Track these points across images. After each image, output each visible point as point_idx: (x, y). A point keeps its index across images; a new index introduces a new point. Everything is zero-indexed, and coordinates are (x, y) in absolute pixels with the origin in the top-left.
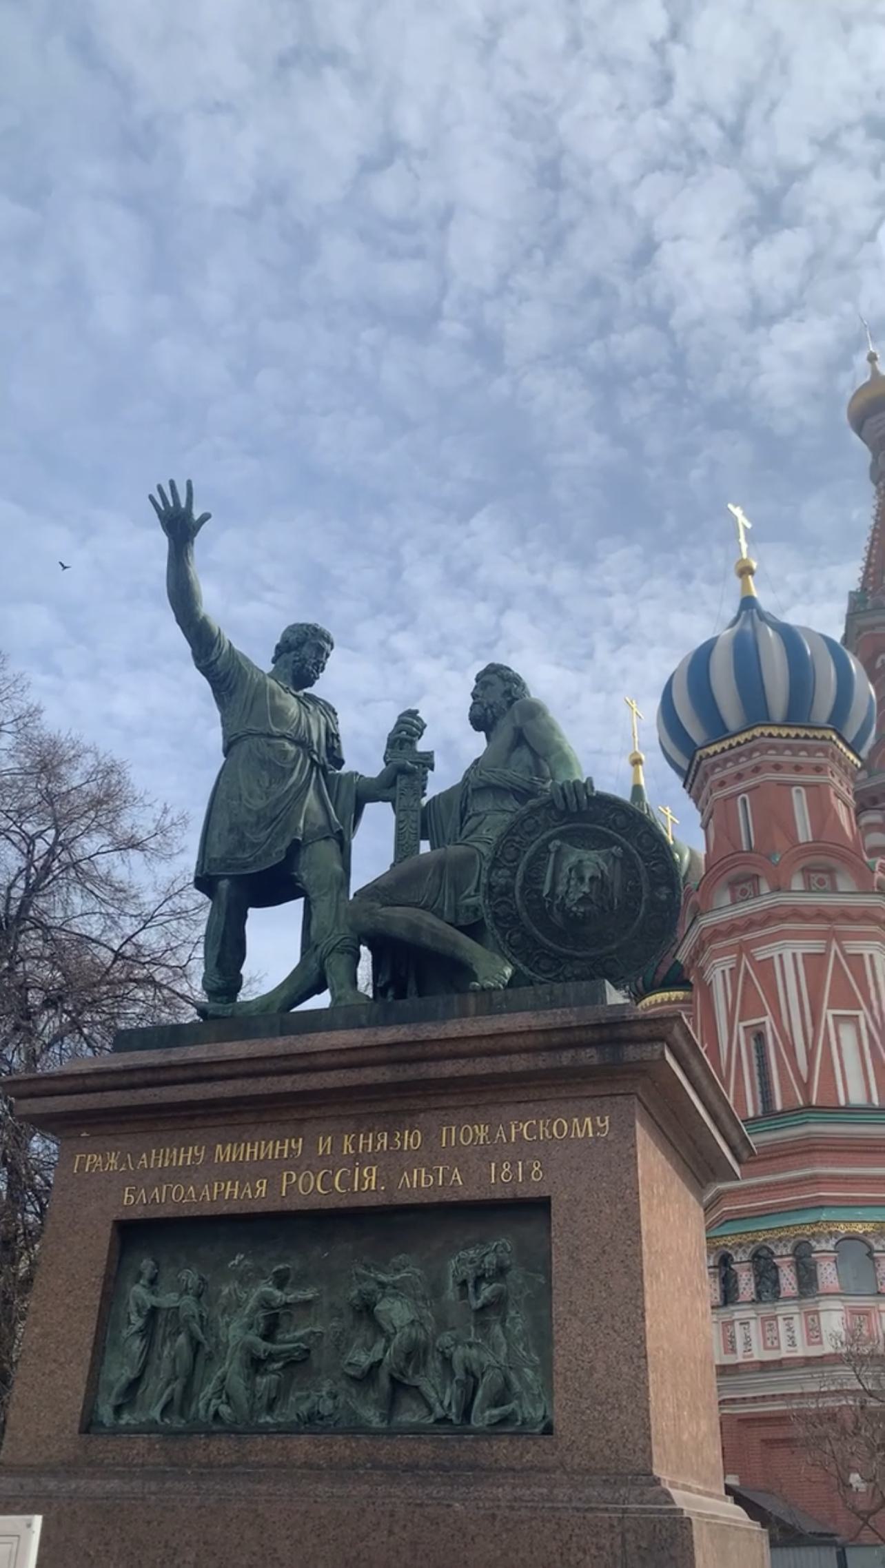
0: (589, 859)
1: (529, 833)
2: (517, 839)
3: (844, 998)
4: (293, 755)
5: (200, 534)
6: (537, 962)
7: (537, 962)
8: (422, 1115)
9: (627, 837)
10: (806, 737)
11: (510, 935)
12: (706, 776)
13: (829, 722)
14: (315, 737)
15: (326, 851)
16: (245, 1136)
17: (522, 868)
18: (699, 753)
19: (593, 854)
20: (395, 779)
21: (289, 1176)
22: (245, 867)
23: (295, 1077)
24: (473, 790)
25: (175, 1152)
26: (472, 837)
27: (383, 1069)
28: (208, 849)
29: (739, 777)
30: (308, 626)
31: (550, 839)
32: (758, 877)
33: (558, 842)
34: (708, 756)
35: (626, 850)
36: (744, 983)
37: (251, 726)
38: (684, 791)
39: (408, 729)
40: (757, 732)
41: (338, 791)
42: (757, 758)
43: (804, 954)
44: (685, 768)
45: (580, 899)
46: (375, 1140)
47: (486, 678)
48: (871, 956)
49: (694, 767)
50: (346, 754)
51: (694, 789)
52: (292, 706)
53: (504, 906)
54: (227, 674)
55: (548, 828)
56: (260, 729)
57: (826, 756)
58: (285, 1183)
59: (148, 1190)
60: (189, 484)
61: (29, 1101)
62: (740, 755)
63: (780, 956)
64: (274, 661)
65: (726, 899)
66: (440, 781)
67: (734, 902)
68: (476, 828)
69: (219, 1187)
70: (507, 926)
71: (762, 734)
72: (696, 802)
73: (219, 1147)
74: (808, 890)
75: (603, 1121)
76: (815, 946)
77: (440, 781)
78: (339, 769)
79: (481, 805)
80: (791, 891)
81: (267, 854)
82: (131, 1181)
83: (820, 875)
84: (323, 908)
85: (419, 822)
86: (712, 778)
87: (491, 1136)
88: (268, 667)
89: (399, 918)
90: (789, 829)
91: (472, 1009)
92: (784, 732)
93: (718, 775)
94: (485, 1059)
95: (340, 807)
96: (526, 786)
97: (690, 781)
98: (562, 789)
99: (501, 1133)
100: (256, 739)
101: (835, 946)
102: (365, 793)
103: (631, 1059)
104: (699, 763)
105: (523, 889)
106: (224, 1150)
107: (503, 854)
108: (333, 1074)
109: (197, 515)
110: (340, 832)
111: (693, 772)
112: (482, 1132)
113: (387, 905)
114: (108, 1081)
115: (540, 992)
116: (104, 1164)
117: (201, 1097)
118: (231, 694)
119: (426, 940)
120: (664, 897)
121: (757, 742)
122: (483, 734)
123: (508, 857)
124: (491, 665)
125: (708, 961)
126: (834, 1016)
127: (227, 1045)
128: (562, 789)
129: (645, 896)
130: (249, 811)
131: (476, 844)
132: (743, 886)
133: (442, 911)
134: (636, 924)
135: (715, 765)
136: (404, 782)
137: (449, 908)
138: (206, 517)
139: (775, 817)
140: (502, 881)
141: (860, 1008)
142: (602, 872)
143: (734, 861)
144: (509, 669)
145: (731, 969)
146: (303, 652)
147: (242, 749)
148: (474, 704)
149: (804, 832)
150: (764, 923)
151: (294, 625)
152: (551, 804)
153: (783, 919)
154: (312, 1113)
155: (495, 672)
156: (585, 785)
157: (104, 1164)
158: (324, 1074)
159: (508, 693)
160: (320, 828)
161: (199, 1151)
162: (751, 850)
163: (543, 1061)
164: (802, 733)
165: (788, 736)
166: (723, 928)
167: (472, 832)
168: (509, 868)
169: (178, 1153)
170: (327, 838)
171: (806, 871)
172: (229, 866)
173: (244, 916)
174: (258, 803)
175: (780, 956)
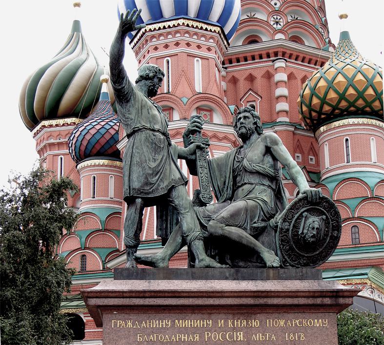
1: (297, 209)
2: (293, 211)
4: (162, 141)
8: (258, 315)
12: (147, 41)
13: (218, 22)
16: (187, 318)
17: (293, 222)
20: (195, 151)
21: (208, 334)
22: (148, 194)
23: (214, 299)
25: (157, 322)
27: (250, 299)
29: (166, 46)
33: (306, 213)
34: (150, 30)
35: (327, 217)
40: (181, 22)
46: (241, 322)
47: (247, 114)
53: (285, 237)
56: (148, 126)
58: (206, 336)
59: (149, 335)
61: (95, 299)
62: (169, 33)
64: (137, 82)
69: (179, 336)
71: (183, 23)
72: (137, 54)
73: (176, 321)
75: (325, 321)
81: (157, 189)
82: (140, 332)
83: (205, 113)
86: (150, 44)
87: (285, 323)
90: (191, 84)
91: (271, 275)
92: (195, 24)
93: (155, 42)
94: (289, 299)
97: (136, 40)
99: (289, 323)
103: (342, 303)
104: (144, 34)
105: (292, 230)
106: (179, 322)
108: (230, 299)
111: (138, 37)
112: (282, 323)
113: (227, 225)
114: (134, 295)
115: (298, 271)
116: (126, 324)
117: (175, 304)
118: (128, 101)
119: (244, 242)
120: (336, 235)
121: (179, 28)
127: (176, 282)
129: (330, 234)
135: (153, 37)
140: (286, 227)
149: (199, 88)
152: (305, 198)
154: (215, 311)
155: (249, 112)
157: (126, 324)
158: (226, 299)
159: (255, 123)
161: (168, 322)
162: (168, 93)
163: (310, 301)
164: (205, 26)
168: (288, 222)
169: (159, 322)
172: (142, 192)
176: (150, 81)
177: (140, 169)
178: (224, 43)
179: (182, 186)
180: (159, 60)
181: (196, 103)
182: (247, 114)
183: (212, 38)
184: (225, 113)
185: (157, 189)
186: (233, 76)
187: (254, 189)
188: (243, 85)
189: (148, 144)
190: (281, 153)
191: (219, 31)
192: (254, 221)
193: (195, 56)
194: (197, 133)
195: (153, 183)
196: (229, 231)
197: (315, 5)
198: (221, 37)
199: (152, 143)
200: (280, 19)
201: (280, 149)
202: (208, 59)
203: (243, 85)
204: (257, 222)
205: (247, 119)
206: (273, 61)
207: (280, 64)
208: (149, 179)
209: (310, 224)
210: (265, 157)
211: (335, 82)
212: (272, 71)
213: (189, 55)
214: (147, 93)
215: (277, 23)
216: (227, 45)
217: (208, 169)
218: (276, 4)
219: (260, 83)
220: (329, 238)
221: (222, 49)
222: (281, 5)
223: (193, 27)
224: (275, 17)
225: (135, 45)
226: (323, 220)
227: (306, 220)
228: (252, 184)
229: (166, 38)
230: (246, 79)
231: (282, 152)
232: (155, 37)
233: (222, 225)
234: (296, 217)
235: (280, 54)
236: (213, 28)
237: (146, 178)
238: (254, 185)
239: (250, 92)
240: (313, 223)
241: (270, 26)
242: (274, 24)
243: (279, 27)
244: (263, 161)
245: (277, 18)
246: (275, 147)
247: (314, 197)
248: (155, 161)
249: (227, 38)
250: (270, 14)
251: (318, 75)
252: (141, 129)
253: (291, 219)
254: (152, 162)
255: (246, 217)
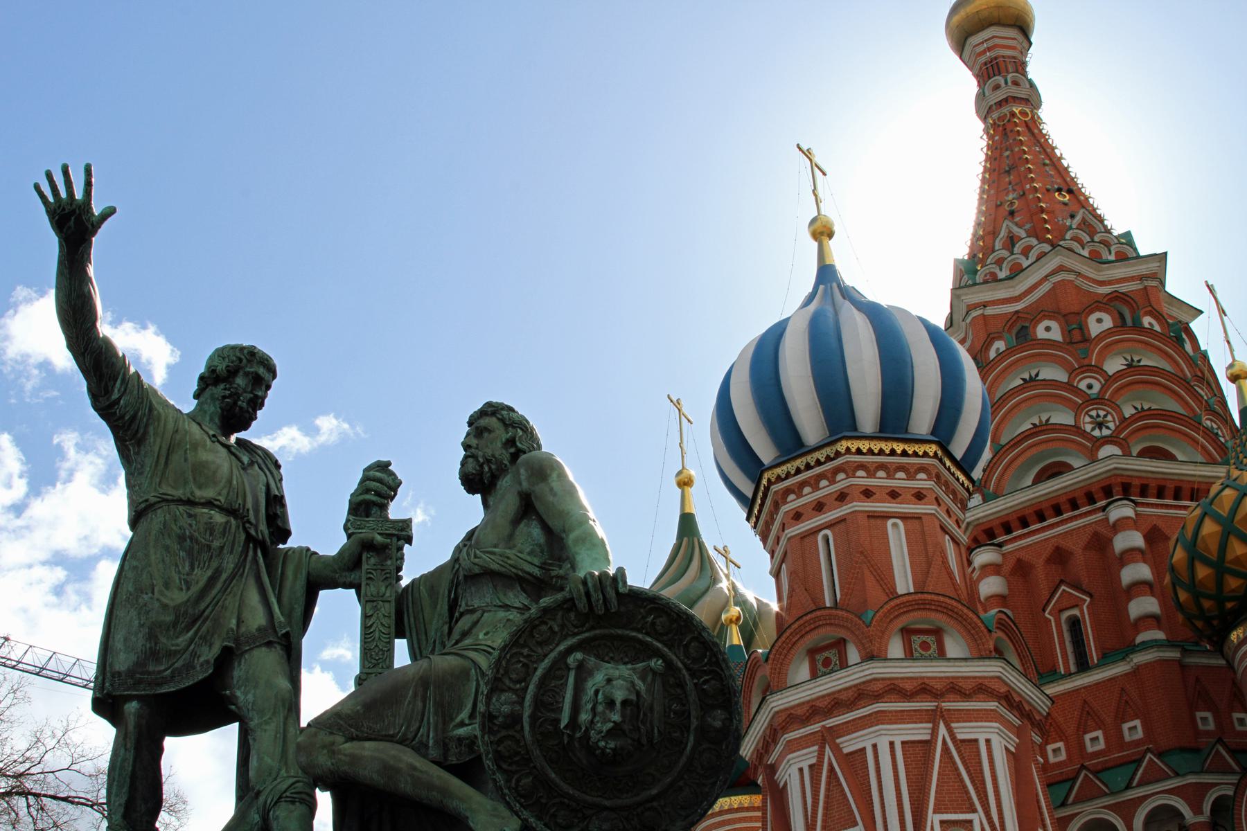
0: (620, 677)
1: (540, 644)
2: (526, 651)
3: (955, 798)
5: (100, 231)
6: (554, 816)
7: (554, 816)
9: (670, 647)
10: (904, 453)
11: (518, 781)
12: (776, 506)
13: (932, 434)
14: (249, 505)
15: (266, 660)
17: (532, 688)
18: (766, 476)
19: (624, 670)
22: (160, 684)
24: (465, 577)
26: (467, 642)
28: (109, 661)
29: (819, 507)
30: (242, 349)
31: (570, 651)
32: (844, 640)
33: (579, 655)
35: (669, 664)
36: (828, 783)
37: (166, 489)
38: (748, 526)
39: (376, 489)
40: (842, 446)
41: (283, 573)
42: (842, 481)
43: (903, 743)
44: (750, 495)
45: (609, 731)
47: (484, 422)
48: (988, 741)
49: (760, 494)
50: (294, 523)
51: (761, 522)
52: (220, 460)
54: (134, 418)
55: (565, 637)
56: (179, 493)
57: (929, 479)
60: (88, 171)
63: (875, 746)
64: (197, 396)
65: (804, 671)
66: (421, 560)
67: (814, 675)
68: (471, 629)
70: (514, 768)
71: (848, 449)
72: (764, 539)
74: (909, 655)
76: (919, 732)
77: (421, 560)
78: (285, 543)
79: (479, 598)
80: (886, 659)
81: (189, 666)
84: (265, 739)
85: (392, 614)
86: (785, 508)
88: (187, 405)
89: (370, 755)
90: (885, 577)
92: (876, 446)
93: (793, 503)
95: (285, 600)
96: (536, 572)
98: (584, 582)
100: (173, 507)
101: (942, 730)
102: (322, 575)
104: (767, 489)
105: (533, 717)
107: (507, 672)
109: (97, 210)
110: (287, 635)
113: (351, 739)
118: (140, 442)
119: (405, 786)
120: (718, 724)
122: (478, 496)
123: (514, 676)
124: (489, 404)
125: (782, 756)
126: (942, 822)
128: (584, 582)
129: (694, 723)
130: (165, 606)
131: (472, 654)
132: (826, 654)
133: (427, 746)
134: (684, 759)
136: (373, 561)
137: (436, 742)
138: (109, 212)
139: (865, 561)
140: (506, 709)
141: (975, 811)
142: (638, 694)
143: (814, 620)
144: (511, 409)
145: (811, 766)
146: (238, 383)
147: (156, 520)
148: (466, 457)
149: (904, 582)
150: (851, 705)
151: (225, 348)
152: (569, 605)
153: (877, 697)
155: (494, 414)
156: (614, 579)
159: (511, 442)
160: (259, 629)
162: (836, 605)
164: (899, 448)
165: (881, 452)
166: (799, 712)
167: (465, 634)
168: (515, 691)
170: (269, 644)
171: (907, 632)
172: (140, 682)
173: (160, 750)
174: (178, 597)
175: (875, 746)
176: (222, 386)
177: (133, 613)
178: (958, 479)
179: (264, 649)
180: (807, 540)
181: (896, 617)
182: (484, 422)
183: (922, 469)
184: (973, 633)
185: (189, 666)
186: (1019, 561)
187: (476, 623)
188: (1042, 576)
189: (168, 542)
190: (551, 499)
191: (935, 453)
192: (458, 719)
193: (887, 516)
194: (374, 510)
195: (176, 652)
196: (353, 756)
197: (1185, 375)
198: (944, 465)
199: (181, 538)
200: (1105, 416)
201: (551, 489)
202: (920, 518)
203: (1042, 576)
204: (467, 721)
205: (486, 435)
206: (1104, 509)
207: (1122, 511)
208: (163, 640)
209: (597, 692)
210: (522, 525)
211: (1238, 518)
212: (1102, 530)
213: (872, 516)
214: (217, 420)
215: (1100, 425)
216: (966, 483)
217: (393, 604)
218: (1090, 387)
219: (1080, 560)
220: (692, 738)
221: (954, 493)
222: (1103, 386)
223: (873, 454)
224: (1094, 413)
225: (758, 518)
226: (654, 673)
227: (585, 680)
228: (472, 611)
229: (816, 488)
230: (1049, 561)
231: (555, 495)
232: (793, 492)
233: (330, 739)
234: (539, 672)
235: (1117, 489)
236: (920, 449)
237: (152, 636)
238: (478, 614)
239: (1063, 587)
240: (614, 679)
241: (1084, 434)
242: (1093, 429)
243: (1106, 432)
244: (511, 536)
245: (1098, 416)
246: (540, 488)
247: (596, 596)
248: (188, 589)
249: (965, 465)
250: (1078, 410)
251: (1198, 512)
252: (151, 505)
253: (524, 680)
254: (176, 592)
255: (424, 707)
